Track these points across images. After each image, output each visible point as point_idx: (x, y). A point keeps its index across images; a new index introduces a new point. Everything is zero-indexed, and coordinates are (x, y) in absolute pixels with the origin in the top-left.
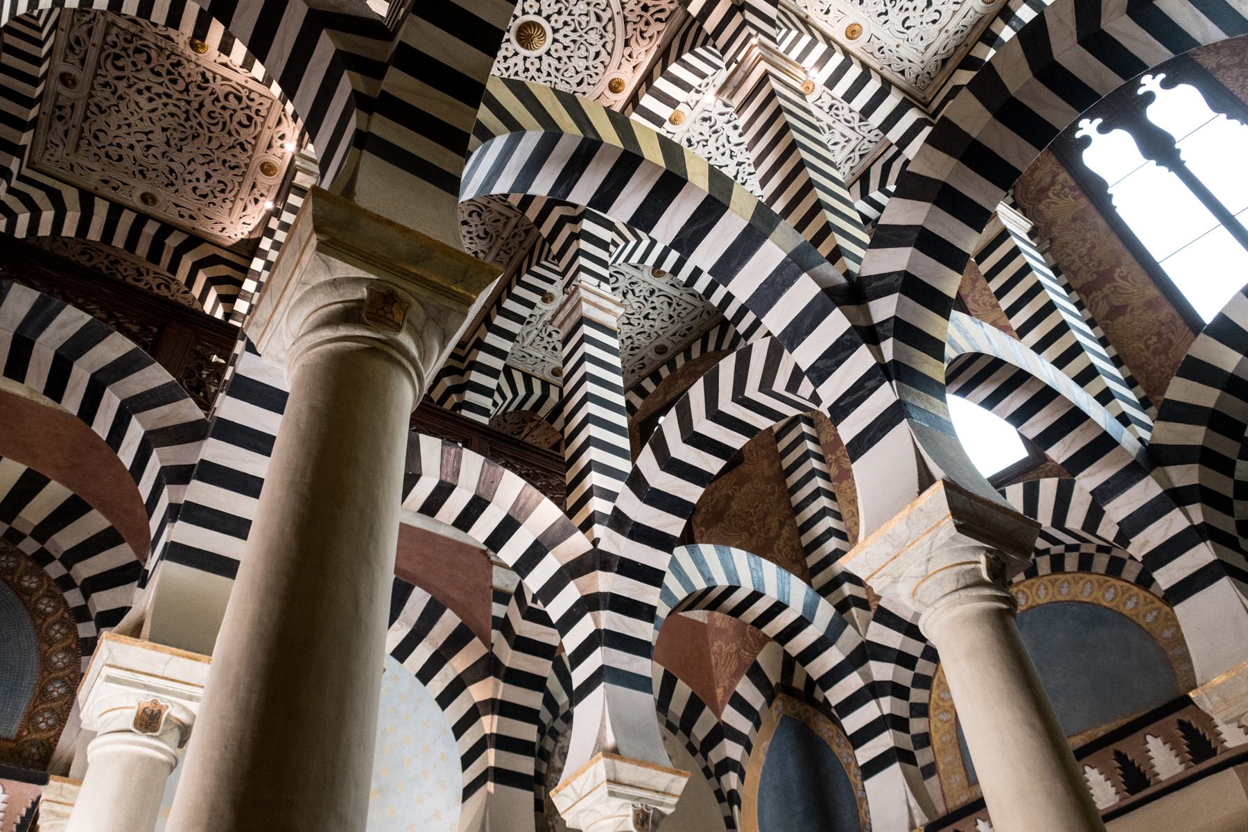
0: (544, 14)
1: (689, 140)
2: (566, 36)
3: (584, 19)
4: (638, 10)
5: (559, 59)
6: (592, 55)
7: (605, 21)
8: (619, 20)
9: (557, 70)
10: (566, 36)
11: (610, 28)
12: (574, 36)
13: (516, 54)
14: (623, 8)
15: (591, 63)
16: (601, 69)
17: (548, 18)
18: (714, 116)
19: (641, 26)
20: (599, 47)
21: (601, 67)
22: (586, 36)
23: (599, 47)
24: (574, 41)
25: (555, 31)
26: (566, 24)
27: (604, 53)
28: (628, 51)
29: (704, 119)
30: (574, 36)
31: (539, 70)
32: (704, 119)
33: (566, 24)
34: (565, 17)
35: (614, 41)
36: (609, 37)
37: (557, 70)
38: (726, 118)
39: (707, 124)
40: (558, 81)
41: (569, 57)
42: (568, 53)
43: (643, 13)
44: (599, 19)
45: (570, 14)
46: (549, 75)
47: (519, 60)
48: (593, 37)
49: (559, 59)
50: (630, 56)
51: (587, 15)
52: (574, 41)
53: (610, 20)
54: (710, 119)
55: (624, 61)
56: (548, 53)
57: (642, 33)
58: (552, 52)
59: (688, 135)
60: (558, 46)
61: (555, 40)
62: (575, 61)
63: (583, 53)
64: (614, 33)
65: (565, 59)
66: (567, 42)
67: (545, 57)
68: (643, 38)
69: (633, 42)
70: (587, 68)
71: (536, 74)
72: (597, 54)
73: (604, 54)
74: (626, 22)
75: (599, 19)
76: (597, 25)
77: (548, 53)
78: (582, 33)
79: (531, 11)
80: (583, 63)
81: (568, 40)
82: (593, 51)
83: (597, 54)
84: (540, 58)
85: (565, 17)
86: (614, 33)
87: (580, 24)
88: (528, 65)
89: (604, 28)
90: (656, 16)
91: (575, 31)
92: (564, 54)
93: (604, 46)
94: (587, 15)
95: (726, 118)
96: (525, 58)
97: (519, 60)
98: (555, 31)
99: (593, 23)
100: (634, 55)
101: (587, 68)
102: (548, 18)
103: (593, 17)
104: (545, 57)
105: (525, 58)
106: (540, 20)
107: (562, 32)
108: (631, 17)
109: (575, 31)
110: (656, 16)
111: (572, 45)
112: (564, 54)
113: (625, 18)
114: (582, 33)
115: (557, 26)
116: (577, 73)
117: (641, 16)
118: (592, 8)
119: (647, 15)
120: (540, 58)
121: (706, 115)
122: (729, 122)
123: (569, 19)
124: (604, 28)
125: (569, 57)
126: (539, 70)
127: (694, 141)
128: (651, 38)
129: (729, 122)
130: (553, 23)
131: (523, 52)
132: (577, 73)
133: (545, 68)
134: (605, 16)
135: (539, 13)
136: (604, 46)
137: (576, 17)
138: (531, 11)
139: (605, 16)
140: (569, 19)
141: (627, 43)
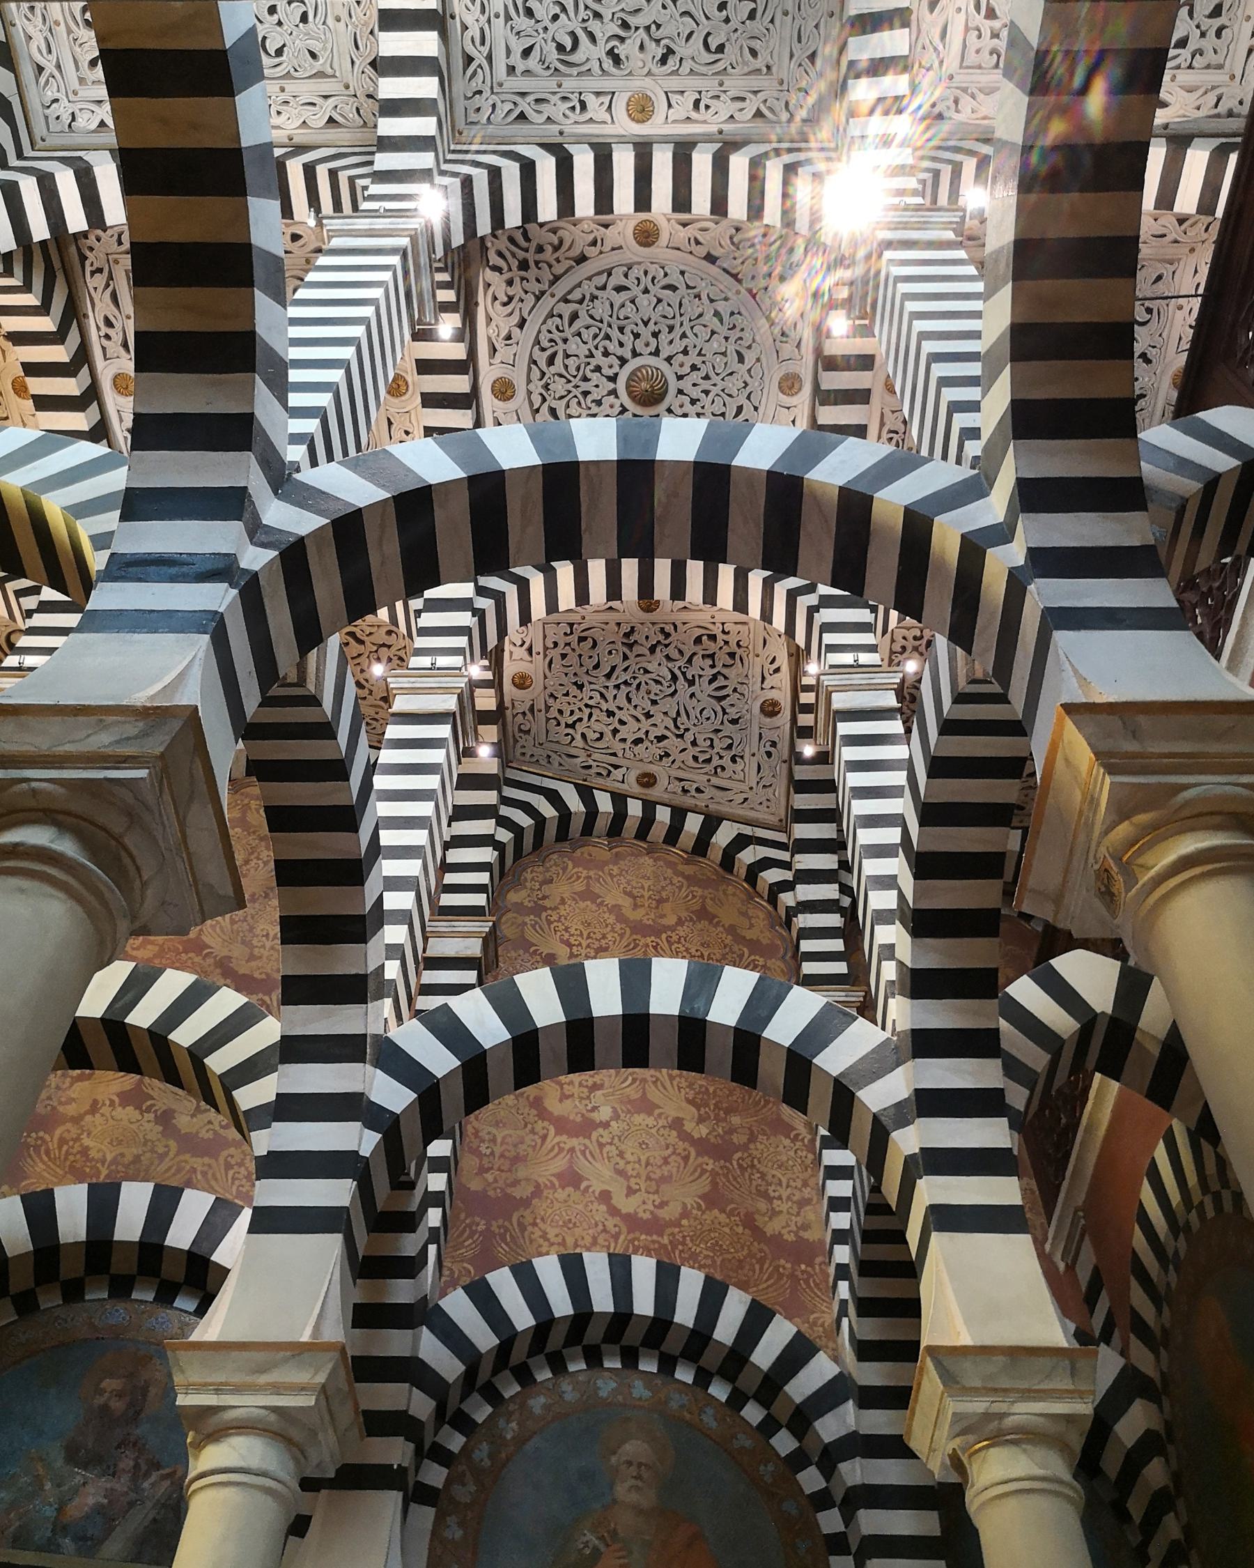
0: (611, 386)
1: (663, 61)
2: (621, 345)
3: (586, 335)
4: (533, 272)
5: (655, 335)
6: (624, 296)
7: (573, 307)
8: (561, 288)
9: (671, 328)
10: (621, 345)
11: (576, 295)
12: (615, 334)
13: (680, 392)
14: (543, 293)
15: (636, 291)
16: (636, 272)
17: (613, 379)
18: (600, 51)
19: (548, 255)
20: (610, 293)
21: (634, 273)
22: (606, 319)
23: (610, 293)
24: (621, 330)
25: (623, 361)
26: (606, 354)
27: (614, 281)
28: (591, 252)
29: (617, 60)
30: (615, 334)
31: (685, 352)
32: (617, 60)
33: (606, 354)
34: (599, 359)
35: (589, 279)
36: (588, 288)
37: (671, 328)
38: (594, 26)
39: (621, 50)
40: (685, 319)
41: (646, 324)
42: (641, 329)
43: (532, 264)
44: (574, 317)
45: (592, 356)
46: (684, 336)
47: (686, 385)
48: (600, 309)
49: (655, 335)
50: (594, 243)
51: (579, 334)
52: (621, 330)
53: (567, 301)
54: (611, 53)
55: (607, 248)
56: (656, 353)
57: (556, 248)
58: (652, 348)
59: (657, 70)
60: (639, 345)
61: (635, 354)
62: (646, 312)
63: (629, 309)
64: (579, 285)
65: (651, 326)
66: (628, 339)
67: (664, 354)
68: (561, 242)
69: (575, 252)
70: (646, 291)
71: (693, 353)
72: (619, 289)
73: (614, 281)
74: (557, 278)
75: (574, 317)
76: (582, 313)
77: (656, 353)
78: (604, 326)
79: (617, 403)
80: (643, 301)
81: (624, 339)
82: (618, 299)
83: (619, 289)
84: (669, 359)
85: (599, 359)
86: (579, 285)
87: (595, 336)
88: (687, 369)
89: (581, 302)
90: (524, 244)
91: (608, 337)
92: (646, 333)
93: (604, 288)
94: (579, 334)
95: (594, 26)
96: (680, 378)
97: (686, 385)
98: (623, 361)
99: (584, 320)
100: (591, 237)
101: (646, 291)
102: (613, 379)
103: (577, 324)
104: (664, 354)
105: (680, 378)
106: (621, 385)
107: (619, 352)
108: (547, 276)
109: (608, 337)
110: (524, 244)
111: (627, 330)
112: (646, 333)
113: (552, 283)
114: (604, 326)
115: (616, 362)
116: (659, 301)
117: (537, 263)
118: (568, 333)
119: (531, 257)
120: (669, 359)
121: (608, 64)
122: (597, 15)
123: (598, 354)
124: (581, 302)
125: (646, 324)
126: (685, 352)
127: (660, 52)
128: (554, 231)
129: (597, 15)
130: (616, 369)
131: (673, 385)
132: (659, 301)
133: (679, 346)
134: (566, 310)
135: (613, 392)
136: (604, 288)
137: (591, 345)
138: (617, 403)
139: (566, 310)
140: (598, 354)
141: (582, 259)
